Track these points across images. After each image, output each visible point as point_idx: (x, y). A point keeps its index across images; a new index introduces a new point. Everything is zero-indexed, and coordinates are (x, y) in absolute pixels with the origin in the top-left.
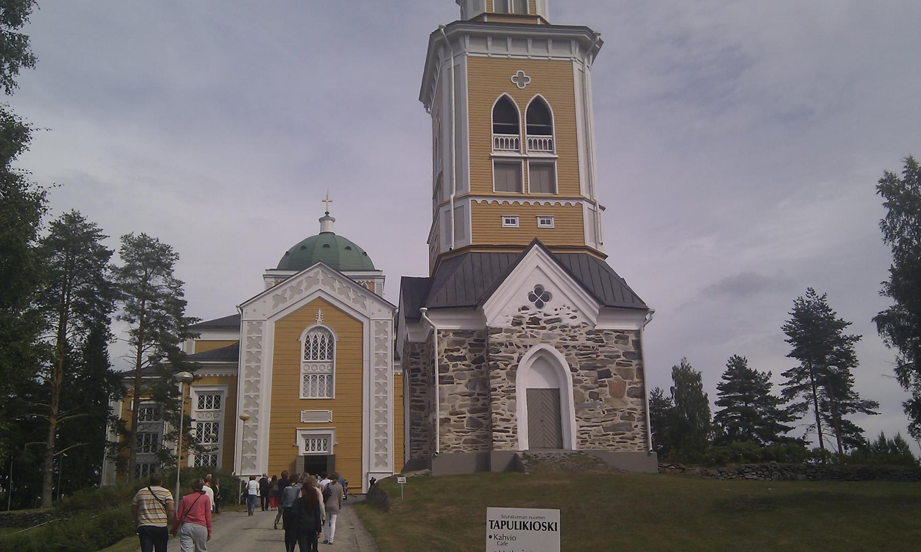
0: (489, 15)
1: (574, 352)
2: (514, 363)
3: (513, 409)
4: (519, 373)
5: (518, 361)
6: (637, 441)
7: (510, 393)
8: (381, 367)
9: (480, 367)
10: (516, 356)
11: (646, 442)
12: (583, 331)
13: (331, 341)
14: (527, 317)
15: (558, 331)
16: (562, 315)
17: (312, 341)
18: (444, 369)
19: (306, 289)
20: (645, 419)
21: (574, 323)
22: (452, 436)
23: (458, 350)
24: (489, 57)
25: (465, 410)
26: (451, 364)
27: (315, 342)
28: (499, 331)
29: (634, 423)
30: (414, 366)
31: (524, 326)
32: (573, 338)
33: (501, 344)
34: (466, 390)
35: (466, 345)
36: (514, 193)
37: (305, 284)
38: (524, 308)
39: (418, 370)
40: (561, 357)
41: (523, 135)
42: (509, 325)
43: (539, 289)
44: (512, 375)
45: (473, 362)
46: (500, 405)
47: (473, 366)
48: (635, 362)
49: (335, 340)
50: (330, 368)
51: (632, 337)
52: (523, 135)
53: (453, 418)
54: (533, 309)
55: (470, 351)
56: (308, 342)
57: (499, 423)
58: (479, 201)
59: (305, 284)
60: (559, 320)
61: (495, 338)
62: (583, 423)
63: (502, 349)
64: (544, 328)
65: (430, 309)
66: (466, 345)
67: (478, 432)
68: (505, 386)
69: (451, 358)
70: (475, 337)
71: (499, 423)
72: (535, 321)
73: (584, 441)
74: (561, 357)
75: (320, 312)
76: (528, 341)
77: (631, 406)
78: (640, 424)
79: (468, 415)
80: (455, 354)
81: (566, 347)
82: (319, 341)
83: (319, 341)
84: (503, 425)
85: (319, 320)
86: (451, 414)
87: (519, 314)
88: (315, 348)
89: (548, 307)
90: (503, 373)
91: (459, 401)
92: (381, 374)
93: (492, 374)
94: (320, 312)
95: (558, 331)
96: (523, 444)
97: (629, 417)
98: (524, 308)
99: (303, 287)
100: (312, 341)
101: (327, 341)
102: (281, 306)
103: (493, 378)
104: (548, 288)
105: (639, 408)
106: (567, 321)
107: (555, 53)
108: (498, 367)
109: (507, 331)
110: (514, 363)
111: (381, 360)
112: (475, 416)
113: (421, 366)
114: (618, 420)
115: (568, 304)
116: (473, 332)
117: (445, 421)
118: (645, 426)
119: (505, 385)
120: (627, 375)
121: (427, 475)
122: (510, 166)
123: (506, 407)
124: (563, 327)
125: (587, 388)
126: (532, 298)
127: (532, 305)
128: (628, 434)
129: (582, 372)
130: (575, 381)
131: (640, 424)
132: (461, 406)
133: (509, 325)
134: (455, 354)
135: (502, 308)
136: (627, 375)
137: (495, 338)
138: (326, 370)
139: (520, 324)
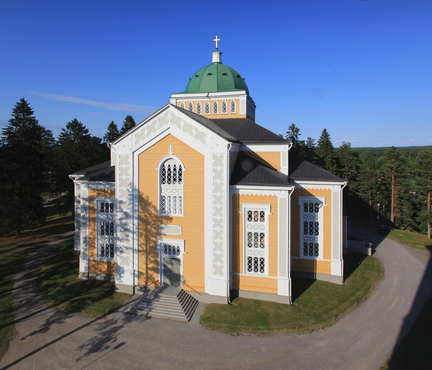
13: (180, 170)
17: (166, 170)
19: (159, 128)
27: (169, 170)
37: (158, 124)
49: (183, 169)
56: (164, 170)
59: (158, 124)
75: (171, 146)
82: (172, 170)
83: (172, 170)
85: (171, 153)
88: (169, 175)
94: (171, 146)
99: (156, 127)
100: (166, 170)
101: (178, 169)
102: (142, 143)
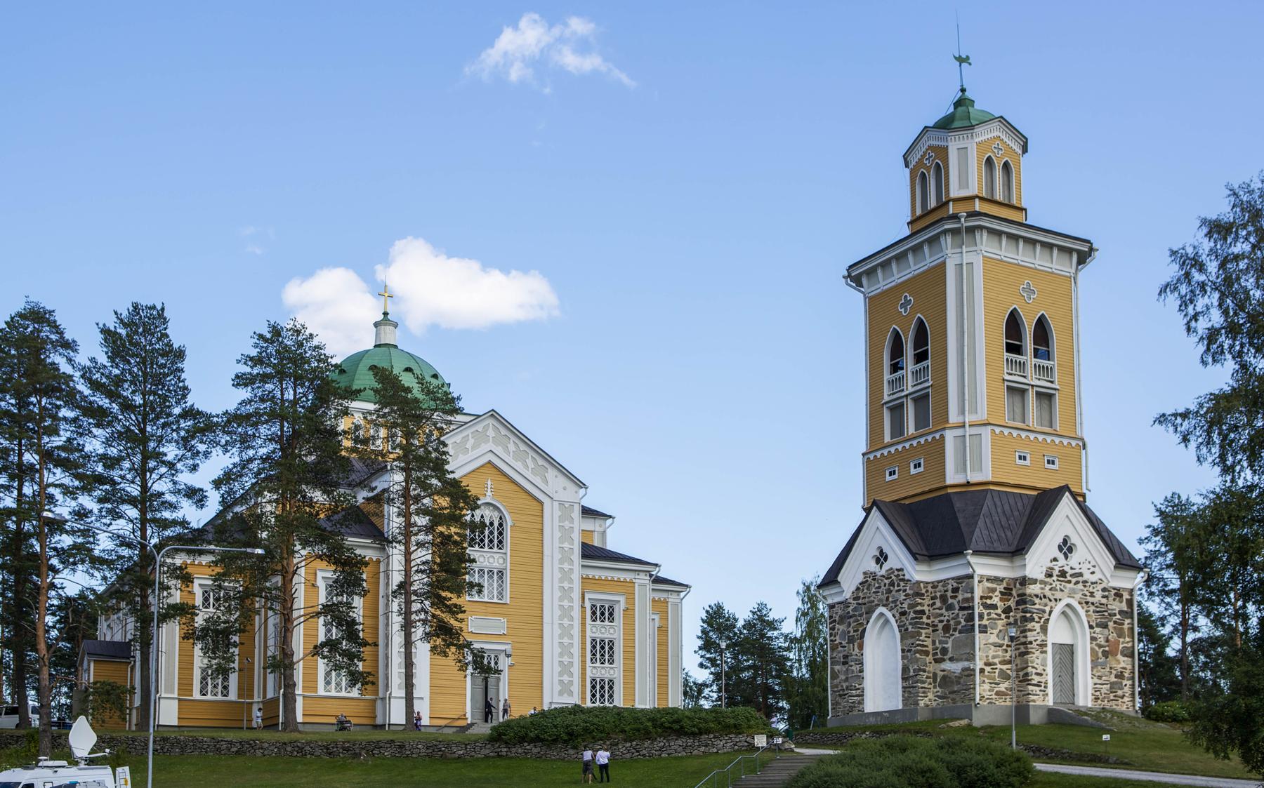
0: (981, 199)
1: (1092, 608)
2: (1046, 616)
3: (1044, 664)
4: (1050, 626)
5: (1051, 612)
6: (1126, 699)
7: (1043, 645)
8: (566, 566)
9: (1008, 617)
10: (1047, 609)
11: (1133, 701)
12: (1100, 587)
14: (1057, 569)
15: (1080, 586)
16: (1085, 571)
18: (981, 617)
20: (1133, 678)
21: (1093, 578)
22: (987, 686)
23: (991, 598)
24: (1001, 261)
25: (996, 661)
26: (985, 612)
28: (1034, 581)
29: (1125, 682)
30: (919, 608)
31: (1055, 578)
32: (1092, 595)
33: (1037, 596)
34: (997, 640)
35: (997, 593)
36: (1021, 425)
38: (1055, 560)
39: (923, 612)
40: (1082, 612)
41: (1028, 358)
42: (1041, 577)
43: (1065, 542)
44: (1044, 629)
45: (1004, 612)
46: (1035, 658)
47: (1003, 616)
48: (1127, 621)
50: (501, 561)
51: (1126, 596)
52: (1028, 358)
53: (988, 669)
54: (1062, 561)
55: (1001, 600)
57: (1034, 676)
58: (998, 430)
60: (1081, 575)
61: (1032, 589)
62: (1096, 680)
63: (1037, 601)
64: (1069, 582)
65: (976, 553)
66: (997, 593)
67: (1007, 684)
68: (1040, 638)
69: (986, 606)
70: (1005, 585)
71: (1034, 676)
72: (1063, 574)
73: (1097, 699)
74: (1082, 612)
76: (1058, 595)
77: (1123, 665)
78: (1130, 682)
79: (999, 666)
80: (989, 602)
81: (1087, 603)
84: (1036, 679)
86: (986, 664)
87: (1051, 565)
89: (1074, 560)
90: (1037, 626)
91: (992, 652)
92: (566, 575)
93: (1030, 626)
95: (1080, 586)
96: (1050, 702)
97: (1120, 676)
98: (1055, 560)
103: (1030, 630)
104: (1074, 539)
105: (1129, 667)
106: (1087, 576)
107: (1038, 259)
108: (1032, 620)
109: (1042, 582)
110: (1046, 616)
111: (566, 557)
112: (1004, 667)
113: (926, 608)
114: (1113, 679)
115: (1090, 558)
116: (1002, 580)
117: (982, 671)
118: (1133, 685)
119: (1040, 639)
120: (1121, 634)
121: (970, 725)
122: (1017, 392)
123: (1039, 661)
124: (1085, 582)
125: (1100, 646)
126: (1060, 549)
127: (1060, 556)
128: (1120, 693)
129: (1098, 630)
130: (1093, 639)
131: (1130, 682)
132: (994, 657)
133: (1041, 577)
134: (989, 602)
135: (1040, 558)
136: (1121, 634)
137: (1032, 589)
138: (496, 564)
139: (1050, 576)
